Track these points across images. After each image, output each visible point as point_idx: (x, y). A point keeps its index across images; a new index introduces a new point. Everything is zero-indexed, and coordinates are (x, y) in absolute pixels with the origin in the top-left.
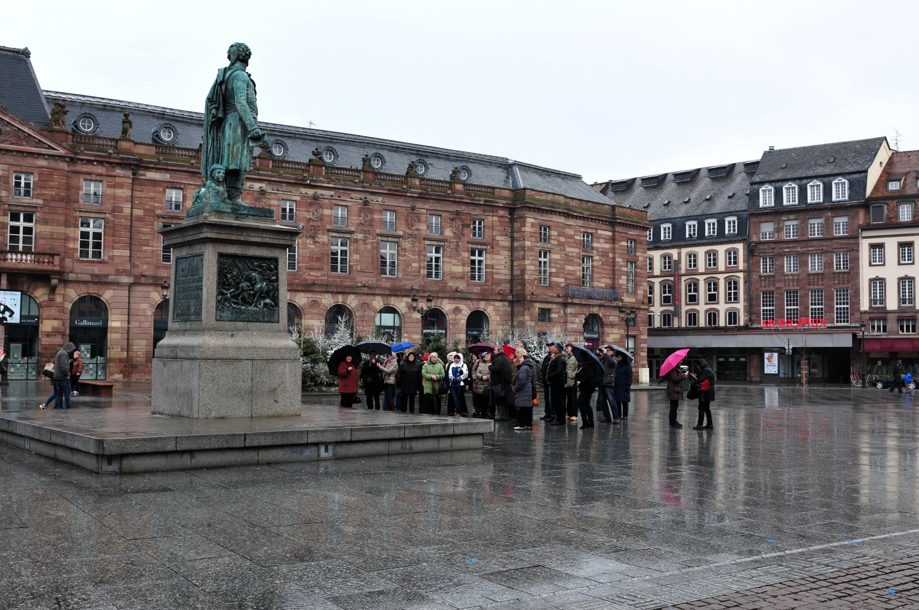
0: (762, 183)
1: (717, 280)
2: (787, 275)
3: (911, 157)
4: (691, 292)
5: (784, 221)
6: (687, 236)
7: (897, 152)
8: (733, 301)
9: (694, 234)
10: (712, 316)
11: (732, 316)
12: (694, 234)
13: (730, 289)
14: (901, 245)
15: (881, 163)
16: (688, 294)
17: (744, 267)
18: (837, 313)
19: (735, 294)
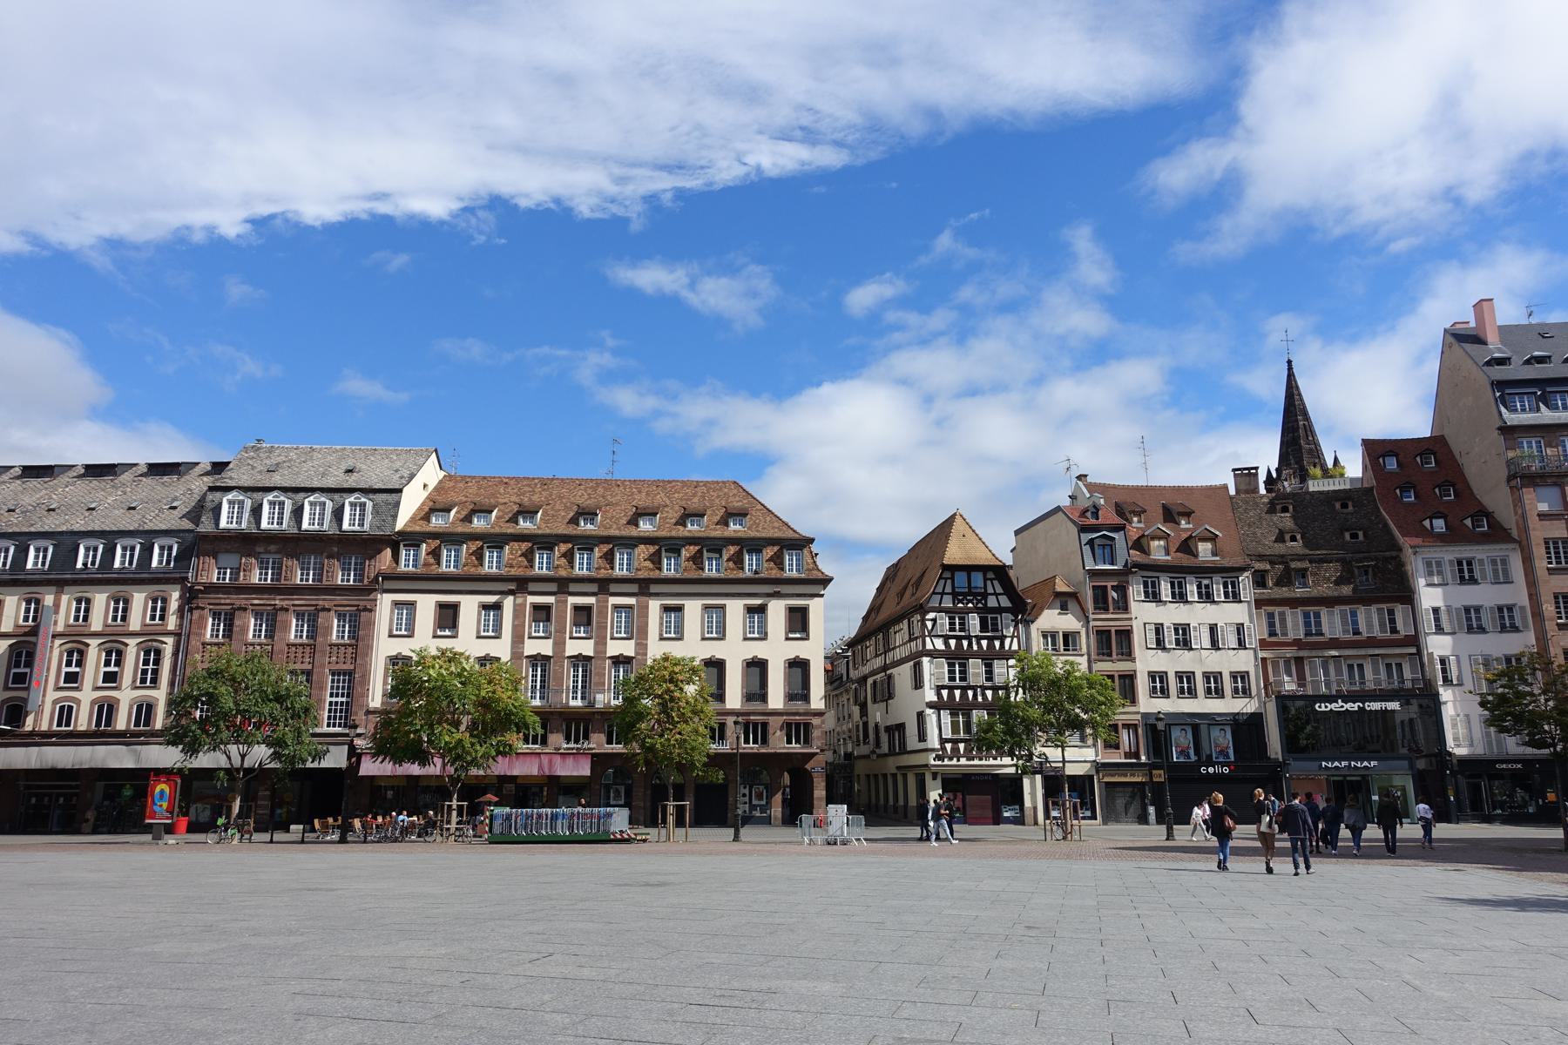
0: (228, 489)
1: (122, 647)
2: (252, 645)
3: (470, 484)
4: (71, 666)
5: (259, 553)
6: (79, 565)
7: (450, 476)
8: (148, 684)
9: (93, 563)
10: (106, 710)
11: (145, 711)
12: (93, 563)
13: (146, 662)
14: (442, 606)
15: (425, 486)
16: (65, 669)
17: (176, 626)
18: (330, 711)
19: (155, 672)
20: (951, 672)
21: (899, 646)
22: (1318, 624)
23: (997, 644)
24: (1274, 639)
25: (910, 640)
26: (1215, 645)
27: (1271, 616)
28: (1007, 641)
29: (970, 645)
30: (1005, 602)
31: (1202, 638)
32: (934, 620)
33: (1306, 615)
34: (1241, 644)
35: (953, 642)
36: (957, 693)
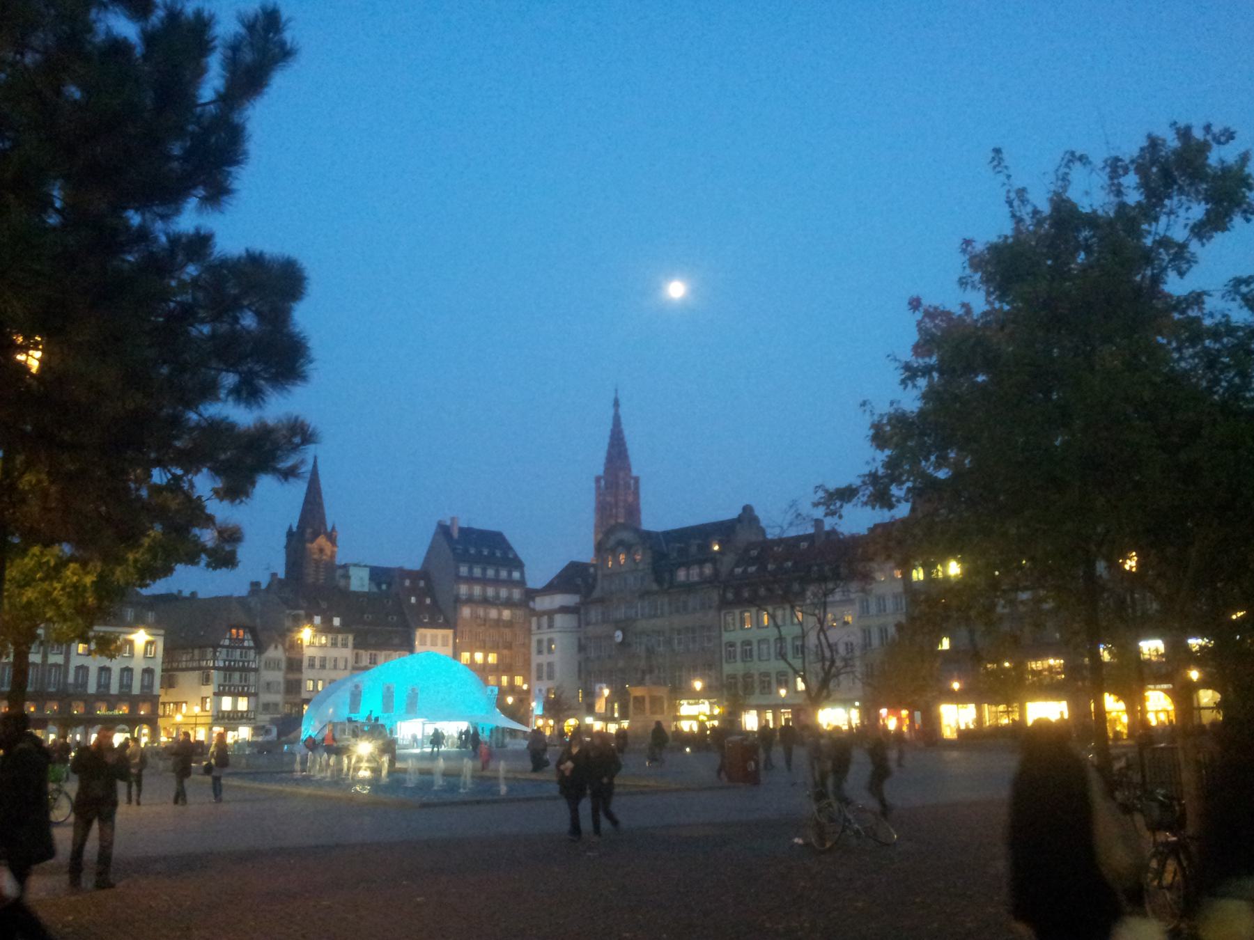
20: (225, 677)
21: (186, 661)
22: (375, 659)
23: (246, 664)
24: (357, 665)
25: (199, 660)
26: (335, 667)
27: (357, 654)
28: (251, 663)
29: (235, 664)
30: (252, 644)
31: (329, 665)
32: (220, 652)
33: (371, 654)
34: (346, 668)
35: (227, 663)
36: (227, 688)
